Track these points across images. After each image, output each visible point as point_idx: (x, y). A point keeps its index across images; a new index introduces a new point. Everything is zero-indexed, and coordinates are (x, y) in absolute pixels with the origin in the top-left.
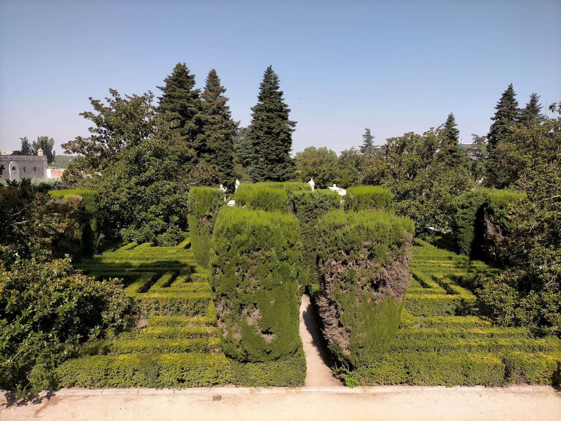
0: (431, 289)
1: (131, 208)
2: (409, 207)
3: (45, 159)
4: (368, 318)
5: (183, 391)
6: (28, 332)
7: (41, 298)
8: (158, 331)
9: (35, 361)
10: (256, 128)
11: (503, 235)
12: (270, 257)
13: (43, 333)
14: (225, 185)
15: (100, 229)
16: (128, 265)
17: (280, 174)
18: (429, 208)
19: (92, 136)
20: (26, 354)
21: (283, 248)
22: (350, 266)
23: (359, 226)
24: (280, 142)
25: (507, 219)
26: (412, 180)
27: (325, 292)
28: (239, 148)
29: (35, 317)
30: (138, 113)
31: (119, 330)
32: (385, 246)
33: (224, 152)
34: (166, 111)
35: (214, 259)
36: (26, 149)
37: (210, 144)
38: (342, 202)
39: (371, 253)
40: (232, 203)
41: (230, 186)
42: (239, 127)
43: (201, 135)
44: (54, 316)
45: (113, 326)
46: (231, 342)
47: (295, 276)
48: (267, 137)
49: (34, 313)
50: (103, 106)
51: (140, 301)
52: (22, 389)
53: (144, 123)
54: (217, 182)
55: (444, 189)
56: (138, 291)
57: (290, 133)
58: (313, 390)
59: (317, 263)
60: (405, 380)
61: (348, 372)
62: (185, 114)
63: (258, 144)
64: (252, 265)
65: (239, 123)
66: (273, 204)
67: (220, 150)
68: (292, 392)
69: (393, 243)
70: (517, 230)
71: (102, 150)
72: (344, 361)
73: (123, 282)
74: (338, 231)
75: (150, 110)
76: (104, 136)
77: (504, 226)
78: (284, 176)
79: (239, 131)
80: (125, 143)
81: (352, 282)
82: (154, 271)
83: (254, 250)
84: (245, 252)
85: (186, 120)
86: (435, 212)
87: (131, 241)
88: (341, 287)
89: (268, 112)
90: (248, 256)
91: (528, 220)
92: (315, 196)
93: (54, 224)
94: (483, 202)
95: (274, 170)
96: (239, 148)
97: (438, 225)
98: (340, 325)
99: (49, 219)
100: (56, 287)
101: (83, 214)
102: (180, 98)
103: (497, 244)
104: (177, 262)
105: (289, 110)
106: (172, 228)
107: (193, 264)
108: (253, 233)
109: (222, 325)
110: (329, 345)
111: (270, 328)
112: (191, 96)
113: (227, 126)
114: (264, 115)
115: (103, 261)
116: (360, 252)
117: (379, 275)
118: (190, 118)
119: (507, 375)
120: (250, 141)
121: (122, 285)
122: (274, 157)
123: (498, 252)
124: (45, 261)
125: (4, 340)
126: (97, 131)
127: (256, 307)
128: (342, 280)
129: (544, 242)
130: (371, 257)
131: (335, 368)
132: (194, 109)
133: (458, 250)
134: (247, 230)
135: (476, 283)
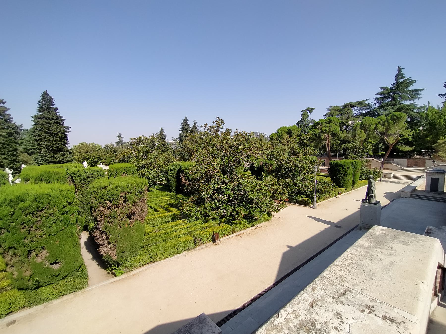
2: (145, 173)
10: (36, 129)
11: (189, 181)
17: (60, 159)
18: (155, 172)
21: (64, 206)
25: (189, 174)
26: (146, 159)
32: (133, 195)
38: (106, 173)
42: (22, 128)
55: (162, 163)
57: (66, 133)
59: (91, 211)
64: (37, 222)
66: (55, 178)
70: (194, 179)
77: (189, 177)
78: (64, 160)
84: (30, 213)
86: (158, 174)
89: (46, 119)
90: (32, 216)
91: (197, 174)
94: (179, 167)
95: (55, 156)
97: (161, 180)
103: (186, 186)
109: (12, 269)
113: (9, 127)
114: (43, 121)
119: (195, 243)
120: (33, 138)
122: (55, 148)
123: (187, 189)
127: (43, 249)
129: (204, 182)
133: (170, 191)
135: (179, 205)
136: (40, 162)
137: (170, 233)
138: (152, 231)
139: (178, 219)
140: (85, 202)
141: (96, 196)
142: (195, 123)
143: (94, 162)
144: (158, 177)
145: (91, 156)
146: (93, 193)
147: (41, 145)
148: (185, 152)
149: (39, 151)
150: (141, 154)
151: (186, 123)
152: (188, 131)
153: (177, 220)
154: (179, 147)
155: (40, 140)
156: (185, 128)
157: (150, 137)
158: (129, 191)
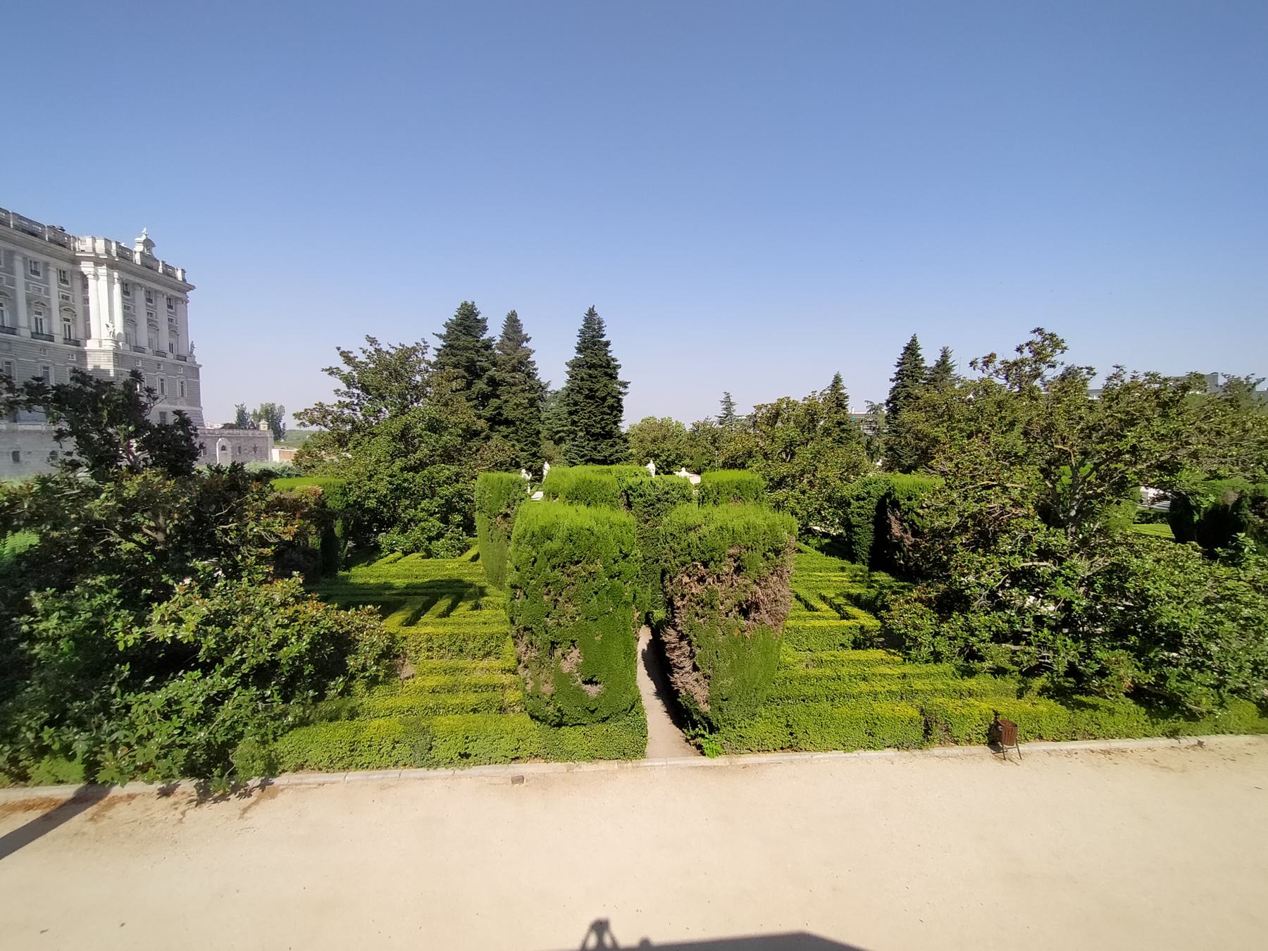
1: (394, 504)
2: (786, 500)
11: (913, 536)
14: (529, 470)
15: (347, 534)
16: (388, 587)
18: (814, 499)
19: (340, 402)
25: (918, 515)
28: (549, 419)
30: (406, 370)
31: (373, 682)
33: (528, 424)
34: (446, 367)
36: (242, 420)
37: (508, 413)
40: (539, 495)
41: (535, 471)
43: (495, 400)
45: (364, 677)
50: (357, 360)
51: (405, 638)
53: (414, 383)
54: (518, 466)
55: (833, 474)
56: (402, 624)
62: (473, 371)
67: (522, 420)
70: (932, 530)
71: (353, 422)
73: (380, 612)
75: (423, 365)
76: (356, 401)
77: (914, 523)
79: (549, 395)
80: (387, 412)
85: (474, 379)
86: (821, 505)
87: (393, 551)
91: (947, 515)
94: (885, 491)
97: (826, 523)
102: (466, 349)
103: (905, 549)
106: (452, 532)
115: (351, 581)
118: (479, 377)
121: (379, 616)
123: (907, 559)
126: (346, 394)
129: (969, 545)
132: (486, 365)
133: (853, 558)
137: (847, 680)
138: (795, 663)
139: (872, 645)
142: (945, 355)
144: (820, 514)
148: (908, 444)
150: (778, 447)
151: (914, 354)
152: (920, 381)
153: (868, 647)
154: (885, 431)
156: (909, 373)
157: (806, 402)
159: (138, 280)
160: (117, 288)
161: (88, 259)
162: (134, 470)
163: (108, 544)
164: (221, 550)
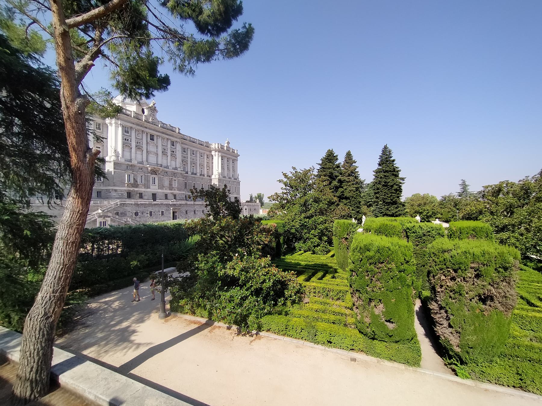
0: (538, 309)
1: (301, 232)
3: (260, 204)
4: (477, 325)
5: (330, 349)
6: (249, 296)
7: (255, 278)
8: (316, 307)
9: (251, 312)
12: (391, 268)
13: (256, 298)
14: (356, 219)
15: (285, 242)
16: (299, 264)
17: (394, 212)
19: (283, 192)
20: (247, 308)
21: (401, 263)
22: (459, 282)
23: (465, 252)
24: (393, 191)
27: (436, 299)
28: (365, 196)
29: (252, 288)
30: (306, 178)
31: (293, 302)
33: (355, 198)
34: (321, 176)
35: (351, 266)
37: (347, 194)
39: (478, 273)
40: (360, 230)
41: (358, 219)
43: (341, 189)
44: (261, 289)
45: (291, 300)
46: (363, 323)
47: (410, 284)
48: (384, 188)
49: (252, 286)
51: (305, 286)
52: (245, 327)
53: (309, 184)
54: (351, 217)
56: (304, 280)
57: (401, 185)
58: (427, 372)
60: (519, 385)
61: (459, 365)
62: (332, 177)
63: (378, 192)
65: (364, 181)
66: (391, 232)
67: (353, 197)
68: (410, 370)
69: (500, 267)
71: (287, 199)
72: (455, 355)
73: (296, 274)
74: (446, 254)
75: (313, 176)
78: (397, 213)
79: (364, 185)
80: (299, 195)
81: (460, 295)
82: (313, 269)
83: (379, 263)
85: (332, 181)
87: (300, 250)
88: (451, 297)
92: (423, 227)
93: (263, 239)
95: (390, 209)
96: (365, 196)
98: (450, 326)
99: (261, 236)
100: (263, 273)
101: (277, 234)
102: (330, 168)
104: (326, 265)
105: (400, 171)
106: (323, 244)
107: (336, 267)
108: (378, 251)
110: (440, 340)
111: (391, 319)
112: (336, 167)
115: (286, 261)
116: (467, 271)
117: (487, 291)
118: (334, 179)
121: (296, 276)
122: (390, 201)
124: (258, 258)
125: (238, 298)
128: (451, 291)
130: (478, 276)
131: (446, 359)
132: (337, 174)
134: (373, 249)
136: (377, 214)
140: (419, 264)
141: (436, 259)
143: (428, 217)
145: (424, 210)
146: (432, 255)
147: (379, 197)
149: (376, 204)
155: (378, 193)
158: (485, 262)
159: (225, 155)
160: (220, 158)
161: (213, 150)
162: (224, 217)
163: (217, 241)
164: (246, 245)
